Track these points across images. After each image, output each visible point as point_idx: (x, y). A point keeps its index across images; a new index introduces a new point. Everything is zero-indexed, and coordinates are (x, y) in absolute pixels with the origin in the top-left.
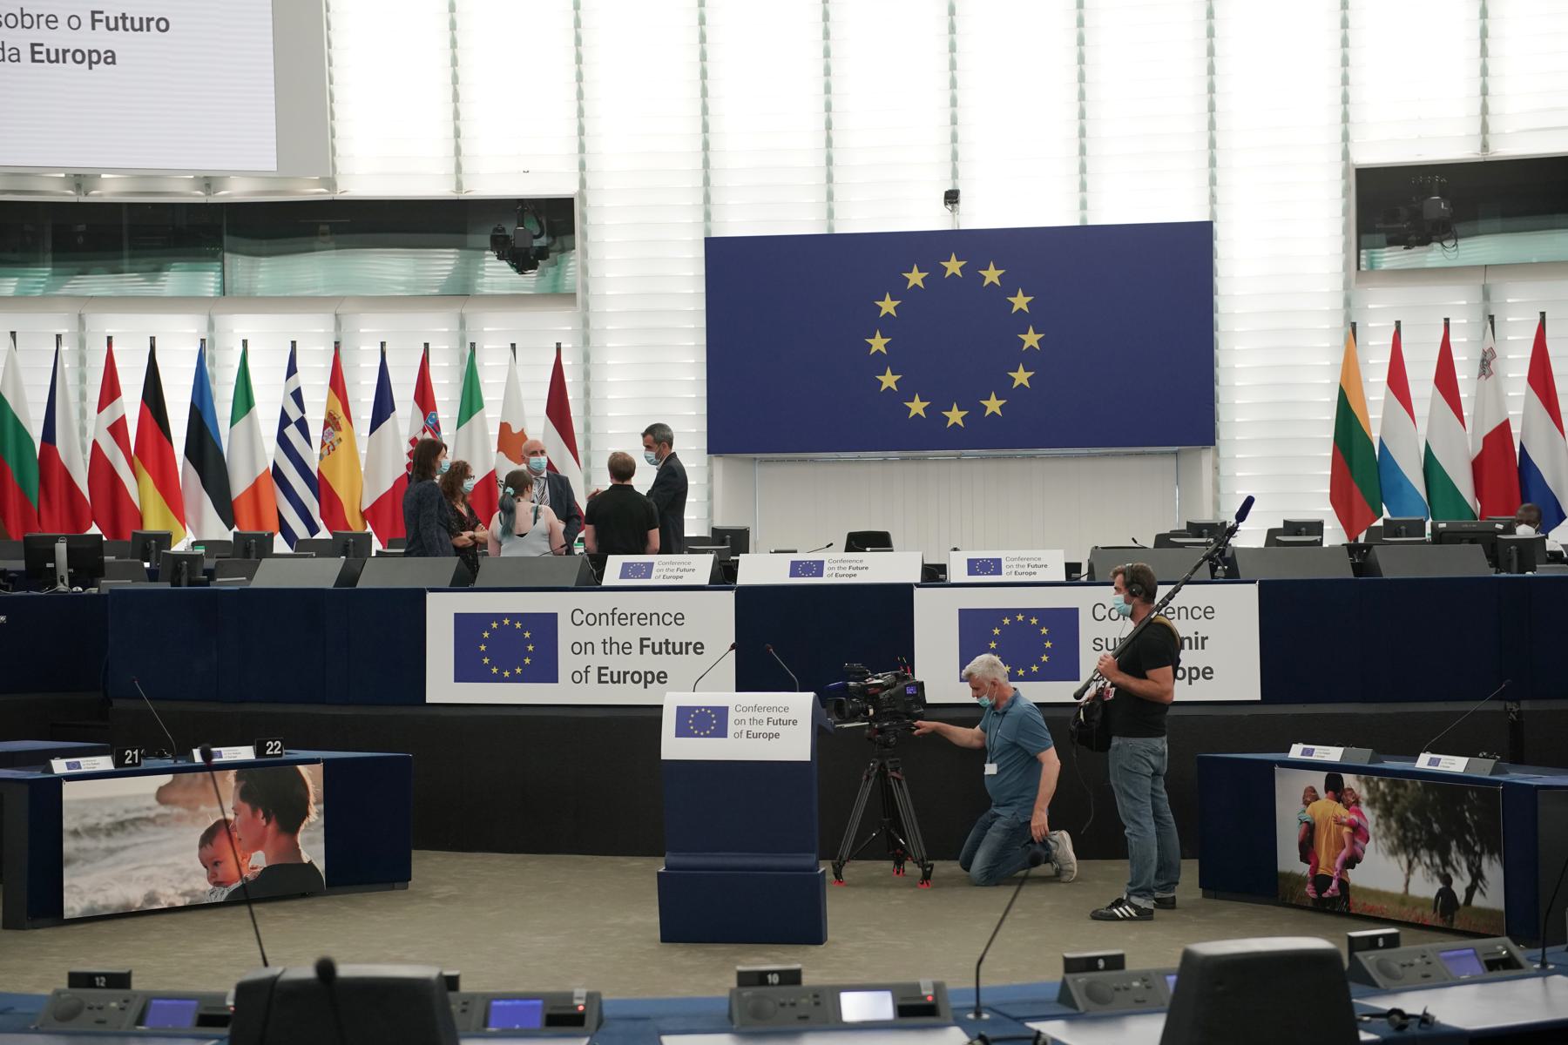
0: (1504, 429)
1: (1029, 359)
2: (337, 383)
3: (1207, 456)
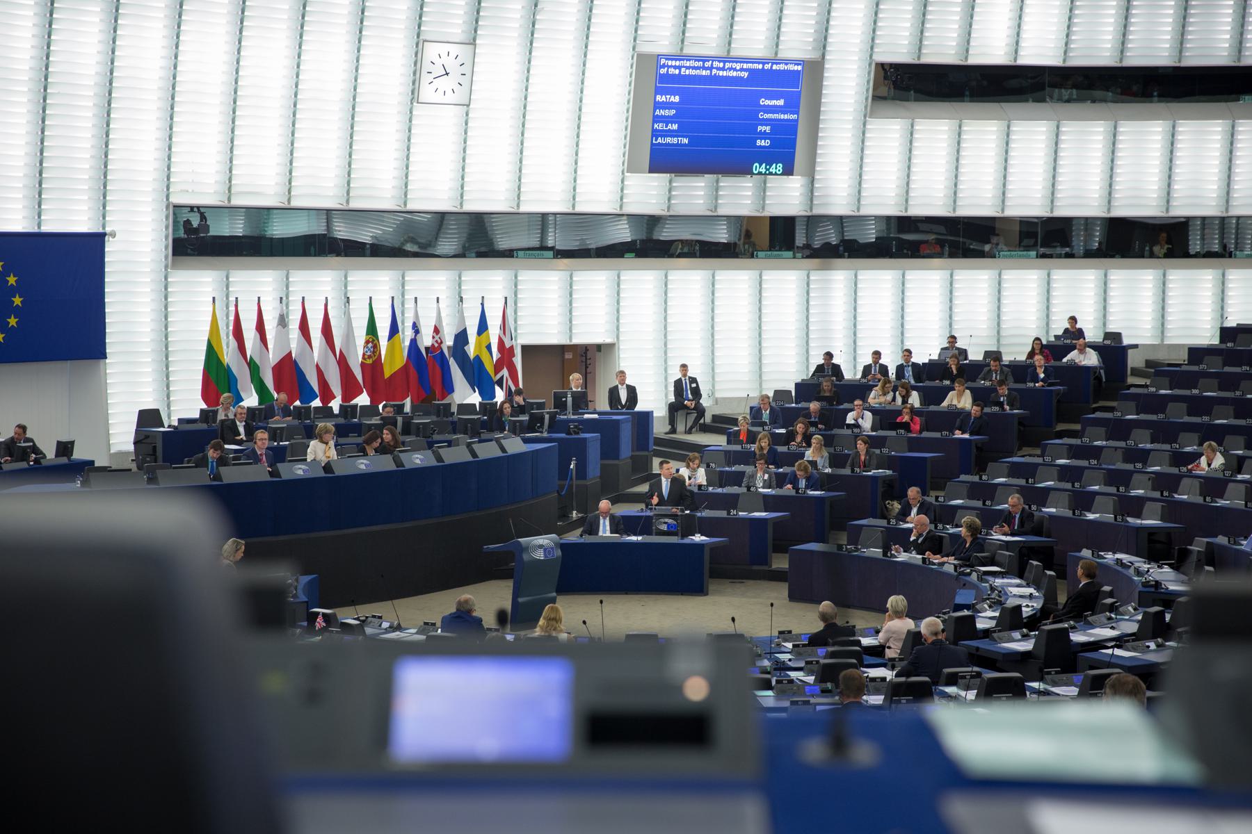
3: (102, 361)
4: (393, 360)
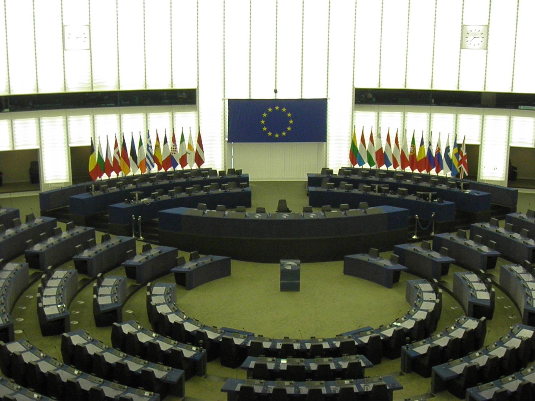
0: (382, 148)
1: (291, 125)
2: (158, 139)
3: (325, 143)
4: (420, 154)
